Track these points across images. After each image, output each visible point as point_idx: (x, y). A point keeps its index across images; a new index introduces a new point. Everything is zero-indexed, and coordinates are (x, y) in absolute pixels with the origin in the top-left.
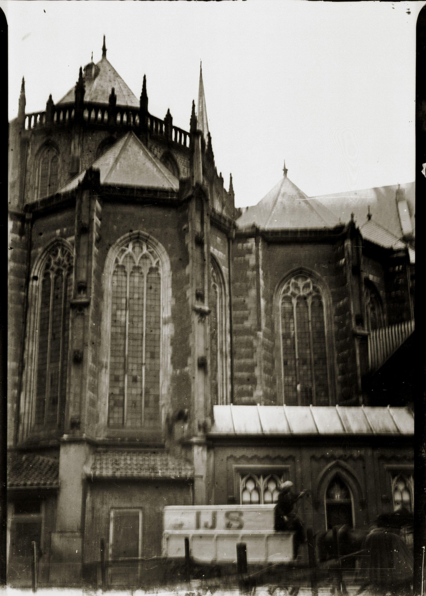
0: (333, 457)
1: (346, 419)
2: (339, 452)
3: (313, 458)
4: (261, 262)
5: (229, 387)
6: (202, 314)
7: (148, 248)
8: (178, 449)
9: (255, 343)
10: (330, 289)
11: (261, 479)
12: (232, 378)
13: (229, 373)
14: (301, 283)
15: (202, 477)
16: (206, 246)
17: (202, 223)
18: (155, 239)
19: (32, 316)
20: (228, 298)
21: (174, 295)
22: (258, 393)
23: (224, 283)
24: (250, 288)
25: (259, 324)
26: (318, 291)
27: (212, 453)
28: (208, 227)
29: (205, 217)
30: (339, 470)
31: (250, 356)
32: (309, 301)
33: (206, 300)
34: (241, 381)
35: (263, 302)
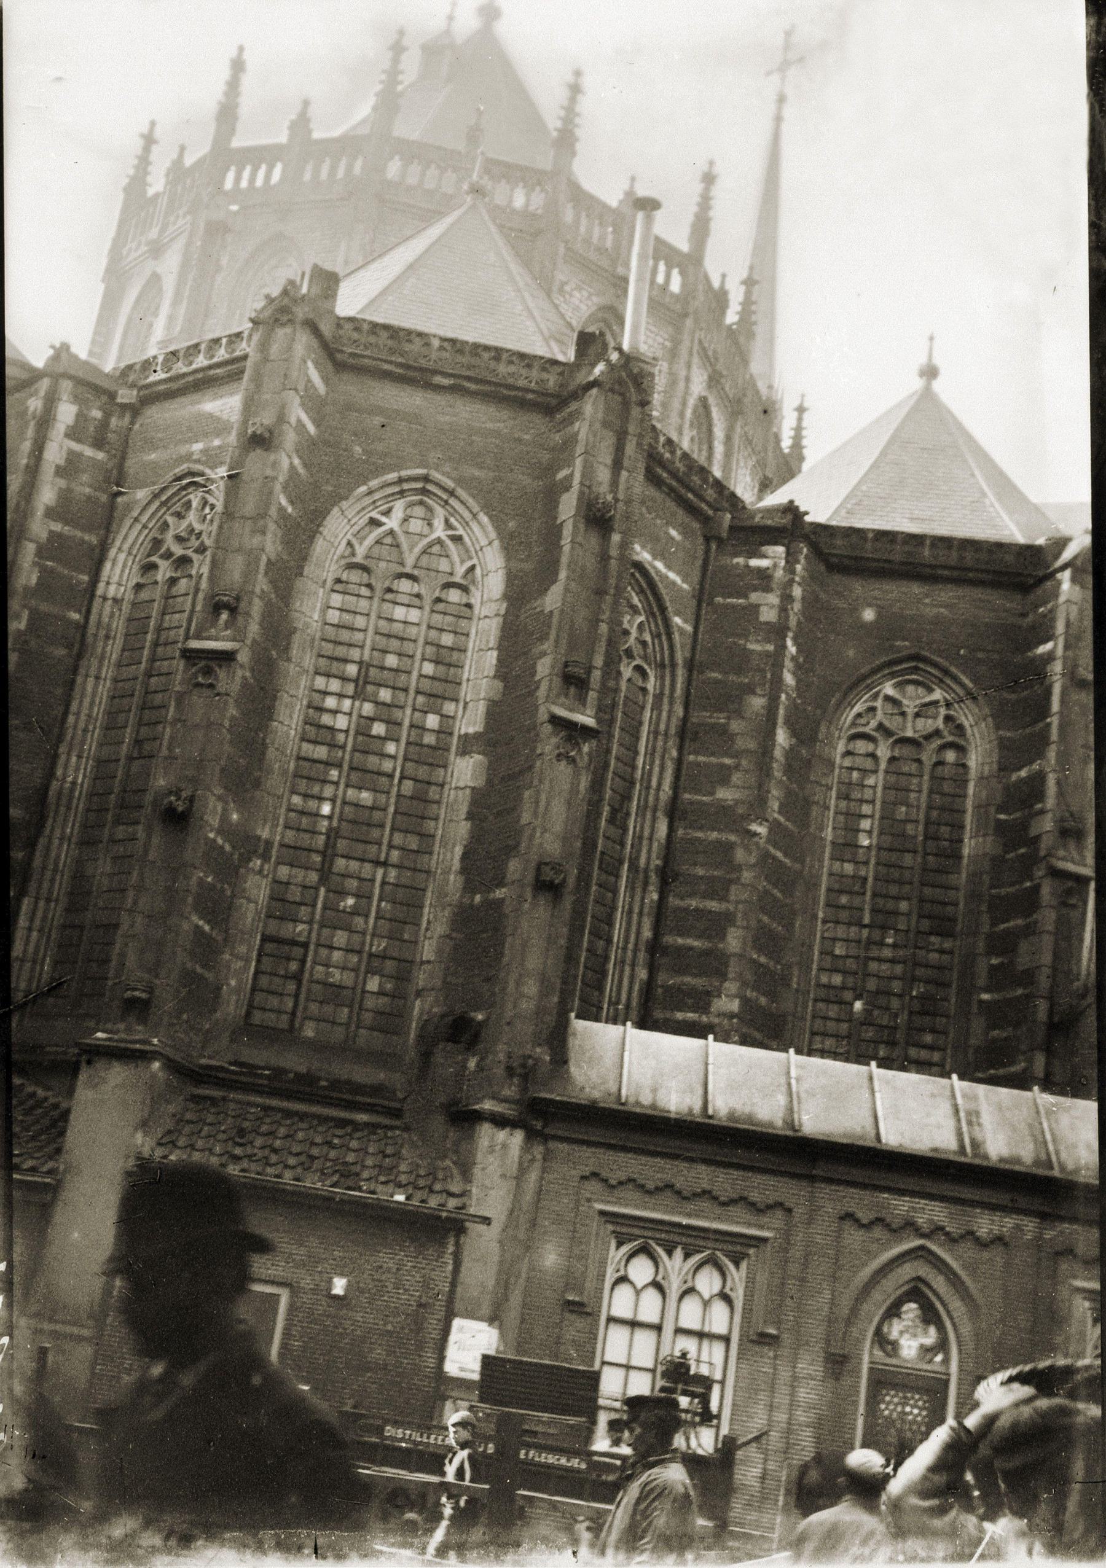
0: (910, 1226)
1: (973, 1117)
2: (931, 1213)
3: (848, 1216)
4: (793, 622)
5: (643, 974)
6: (572, 732)
7: (448, 525)
8: (438, 1123)
9: (740, 855)
10: (997, 727)
11: (678, 1253)
12: (655, 947)
13: (647, 934)
14: (912, 698)
15: (487, 1221)
16: (616, 538)
17: (617, 465)
18: (471, 502)
19: (91, 681)
20: (679, 711)
21: (503, 671)
22: (728, 1004)
23: (673, 665)
24: (750, 690)
25: (762, 801)
26: (960, 728)
27: (538, 1150)
28: (634, 482)
29: (630, 448)
30: (923, 1270)
31: (718, 889)
32: (928, 756)
33: (592, 695)
34: (683, 960)
35: (782, 737)
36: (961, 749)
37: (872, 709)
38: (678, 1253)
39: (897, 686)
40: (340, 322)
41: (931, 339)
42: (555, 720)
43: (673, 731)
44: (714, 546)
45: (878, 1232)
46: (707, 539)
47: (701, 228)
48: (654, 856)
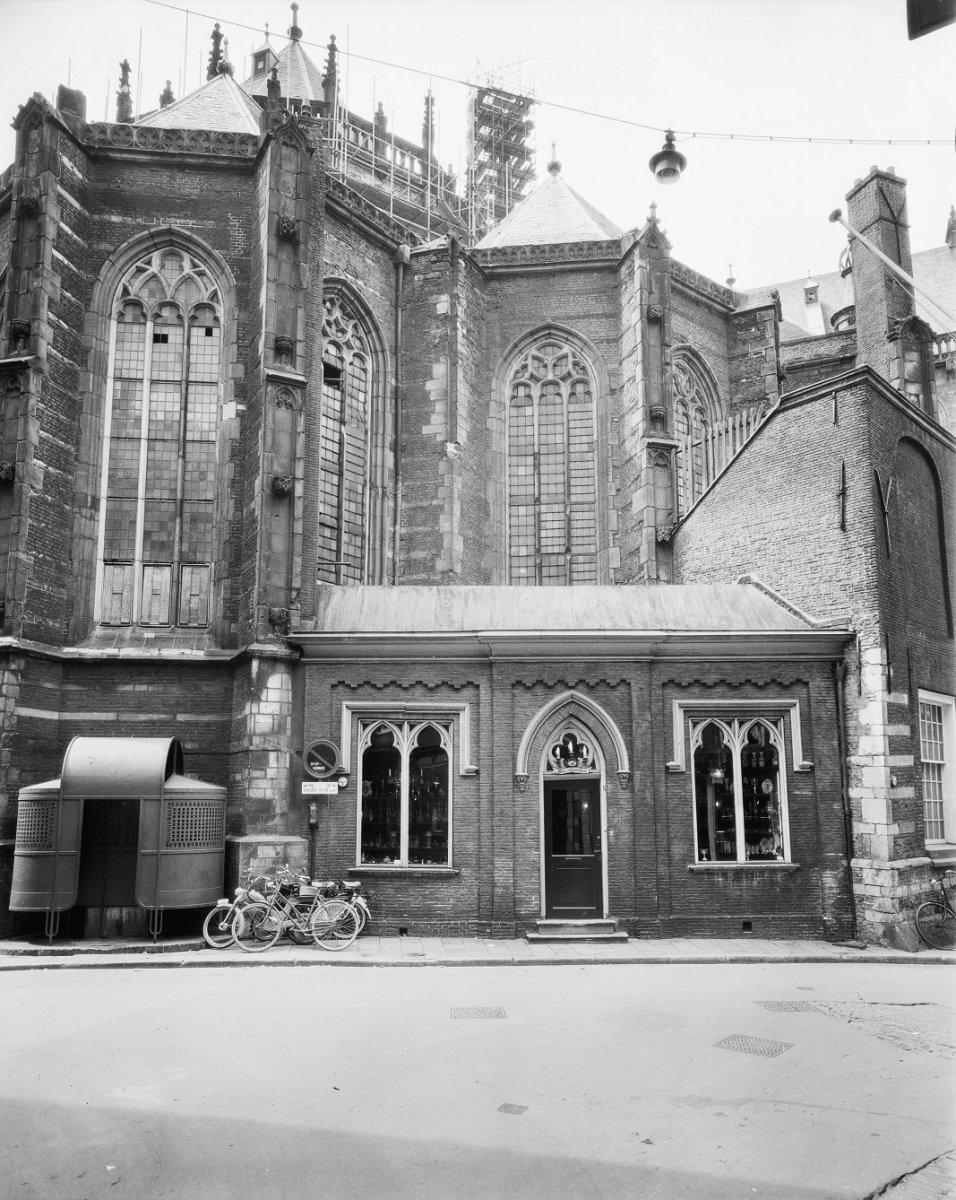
3: (519, 683)
7: (195, 266)
23: (383, 351)
36: (585, 382)
37: (525, 367)
38: (406, 727)
39: (539, 349)
40: (88, 129)
41: (553, 146)
42: (272, 379)
43: (388, 394)
44: (401, 271)
45: (539, 690)
46: (396, 267)
47: (428, 133)
48: (386, 477)
